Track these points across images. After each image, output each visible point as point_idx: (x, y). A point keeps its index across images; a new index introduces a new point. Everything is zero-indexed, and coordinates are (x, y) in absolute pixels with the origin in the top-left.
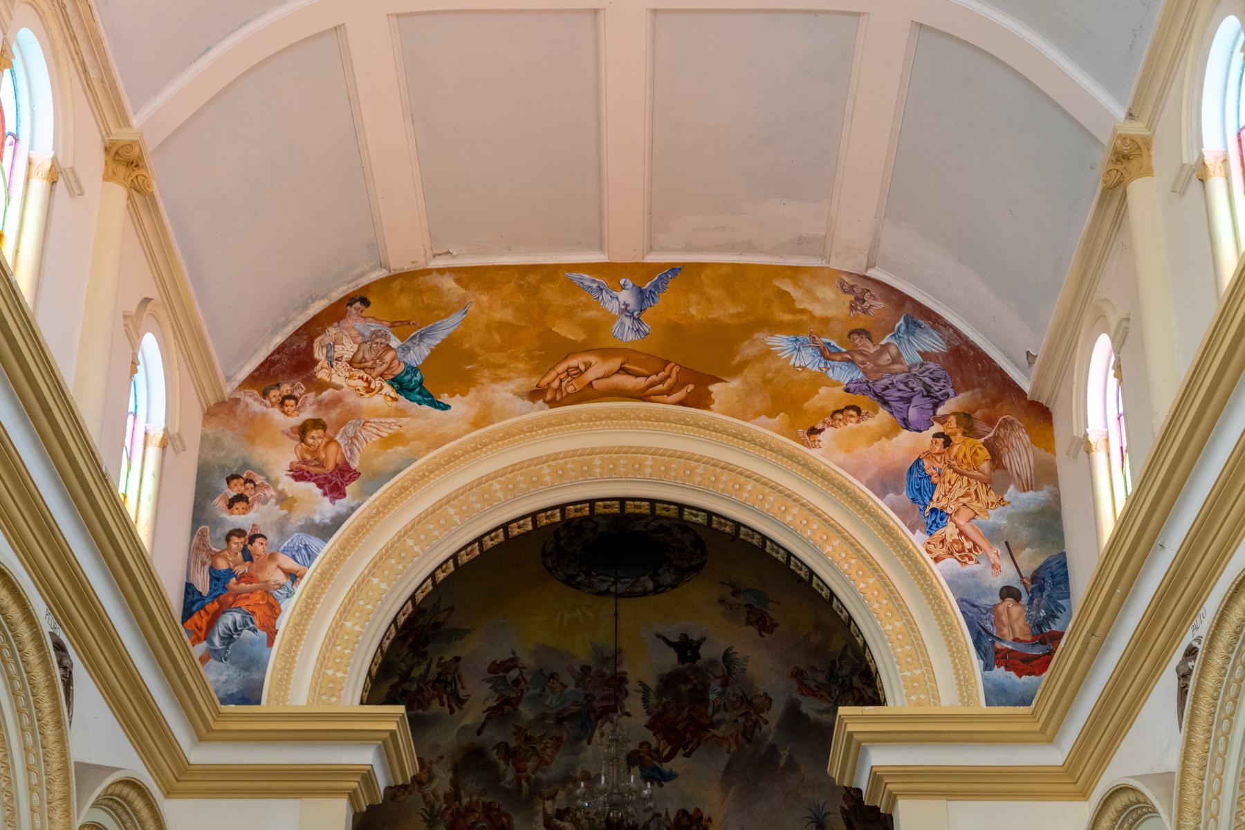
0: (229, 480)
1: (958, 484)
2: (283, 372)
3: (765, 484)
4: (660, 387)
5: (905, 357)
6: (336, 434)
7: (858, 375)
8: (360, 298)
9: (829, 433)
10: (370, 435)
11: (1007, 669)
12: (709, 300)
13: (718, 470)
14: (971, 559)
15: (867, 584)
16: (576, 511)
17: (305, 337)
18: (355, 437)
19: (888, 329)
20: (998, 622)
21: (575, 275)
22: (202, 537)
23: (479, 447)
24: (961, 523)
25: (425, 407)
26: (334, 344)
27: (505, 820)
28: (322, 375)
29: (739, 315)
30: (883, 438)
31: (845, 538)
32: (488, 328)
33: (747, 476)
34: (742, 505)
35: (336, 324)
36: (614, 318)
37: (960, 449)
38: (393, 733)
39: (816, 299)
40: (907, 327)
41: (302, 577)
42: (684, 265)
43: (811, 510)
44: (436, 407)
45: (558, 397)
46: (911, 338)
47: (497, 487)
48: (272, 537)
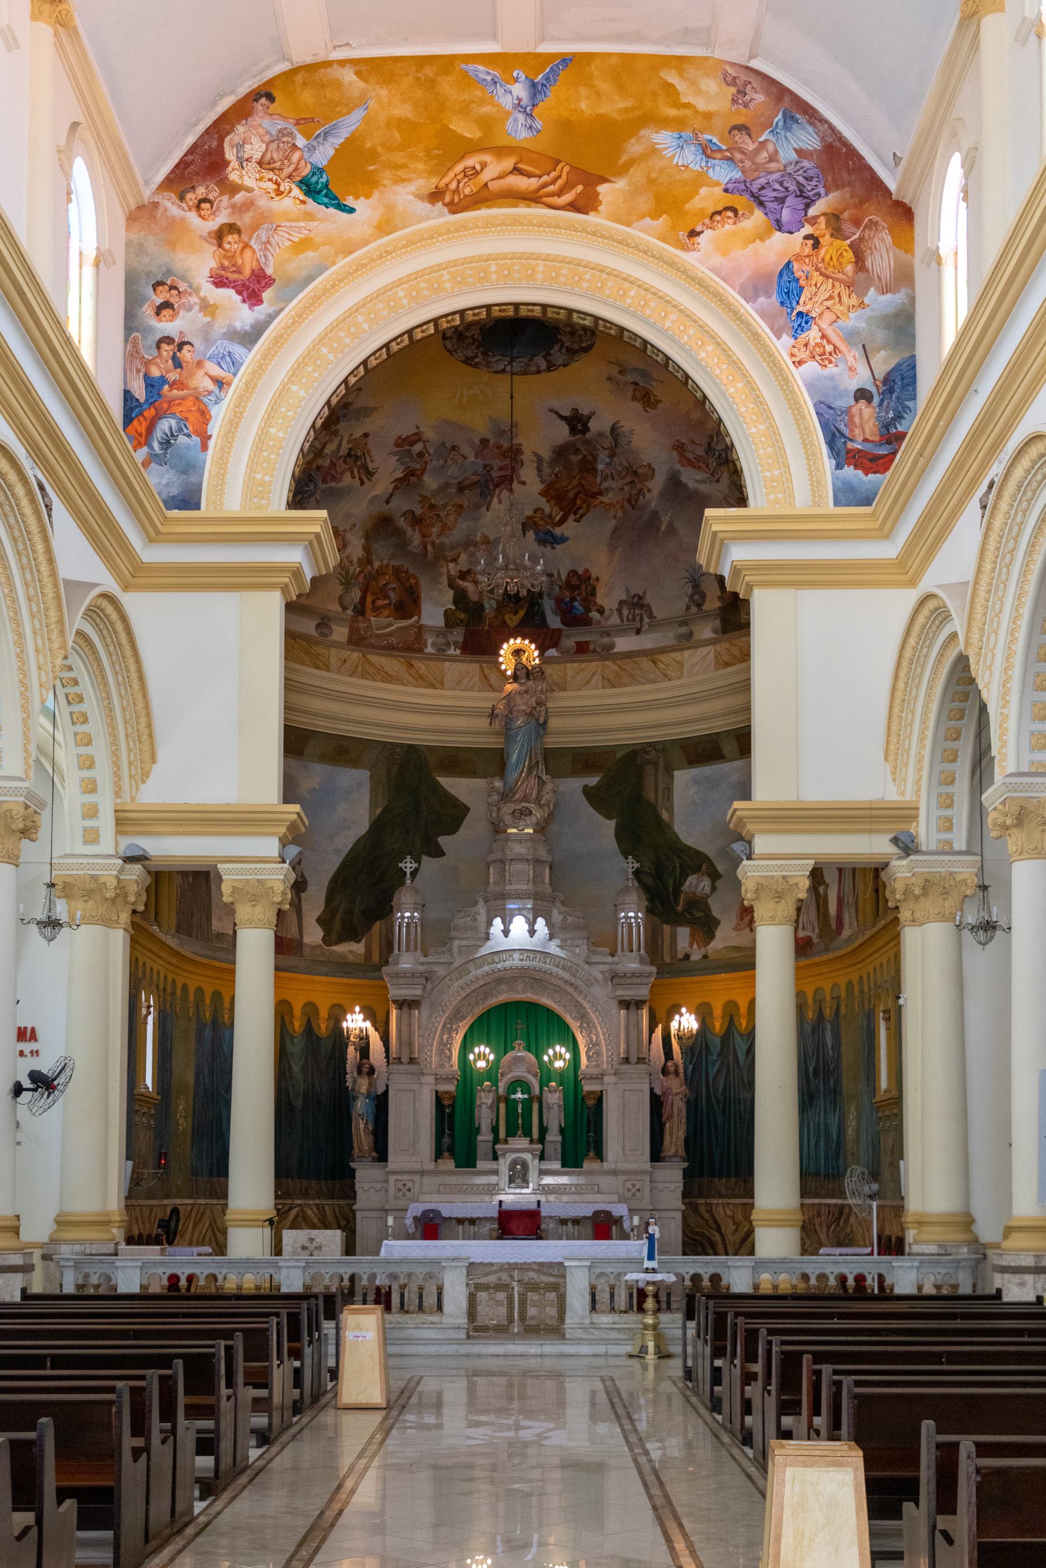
0: (155, 286)
1: (823, 288)
2: (197, 174)
3: (647, 290)
4: (551, 188)
5: (781, 154)
6: (250, 239)
7: (737, 175)
8: (265, 94)
9: (708, 234)
10: (282, 240)
11: (856, 467)
12: (598, 94)
13: (605, 276)
14: (830, 362)
15: (735, 389)
16: (474, 315)
17: (216, 136)
18: (268, 242)
19: (767, 125)
20: (850, 425)
21: (471, 67)
22: (135, 345)
23: (385, 254)
24: (824, 325)
25: (332, 211)
26: (244, 143)
27: (413, 581)
28: (234, 176)
29: (626, 110)
30: (758, 241)
31: (718, 344)
32: (389, 125)
33: (631, 283)
34: (625, 311)
35: (244, 122)
36: (508, 114)
37: (827, 251)
38: (317, 535)
39: (699, 92)
40: (785, 122)
41: (229, 384)
42: (575, 54)
43: (688, 316)
44: (343, 211)
45: (456, 200)
46: (788, 134)
47: (401, 294)
48: (198, 343)
